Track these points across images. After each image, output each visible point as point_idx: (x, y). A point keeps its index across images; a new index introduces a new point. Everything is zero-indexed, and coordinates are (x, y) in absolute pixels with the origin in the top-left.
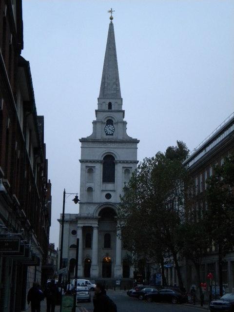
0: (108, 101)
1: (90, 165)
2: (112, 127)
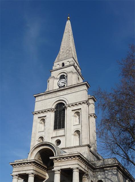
0: (61, 63)
1: (42, 115)
2: (64, 80)
